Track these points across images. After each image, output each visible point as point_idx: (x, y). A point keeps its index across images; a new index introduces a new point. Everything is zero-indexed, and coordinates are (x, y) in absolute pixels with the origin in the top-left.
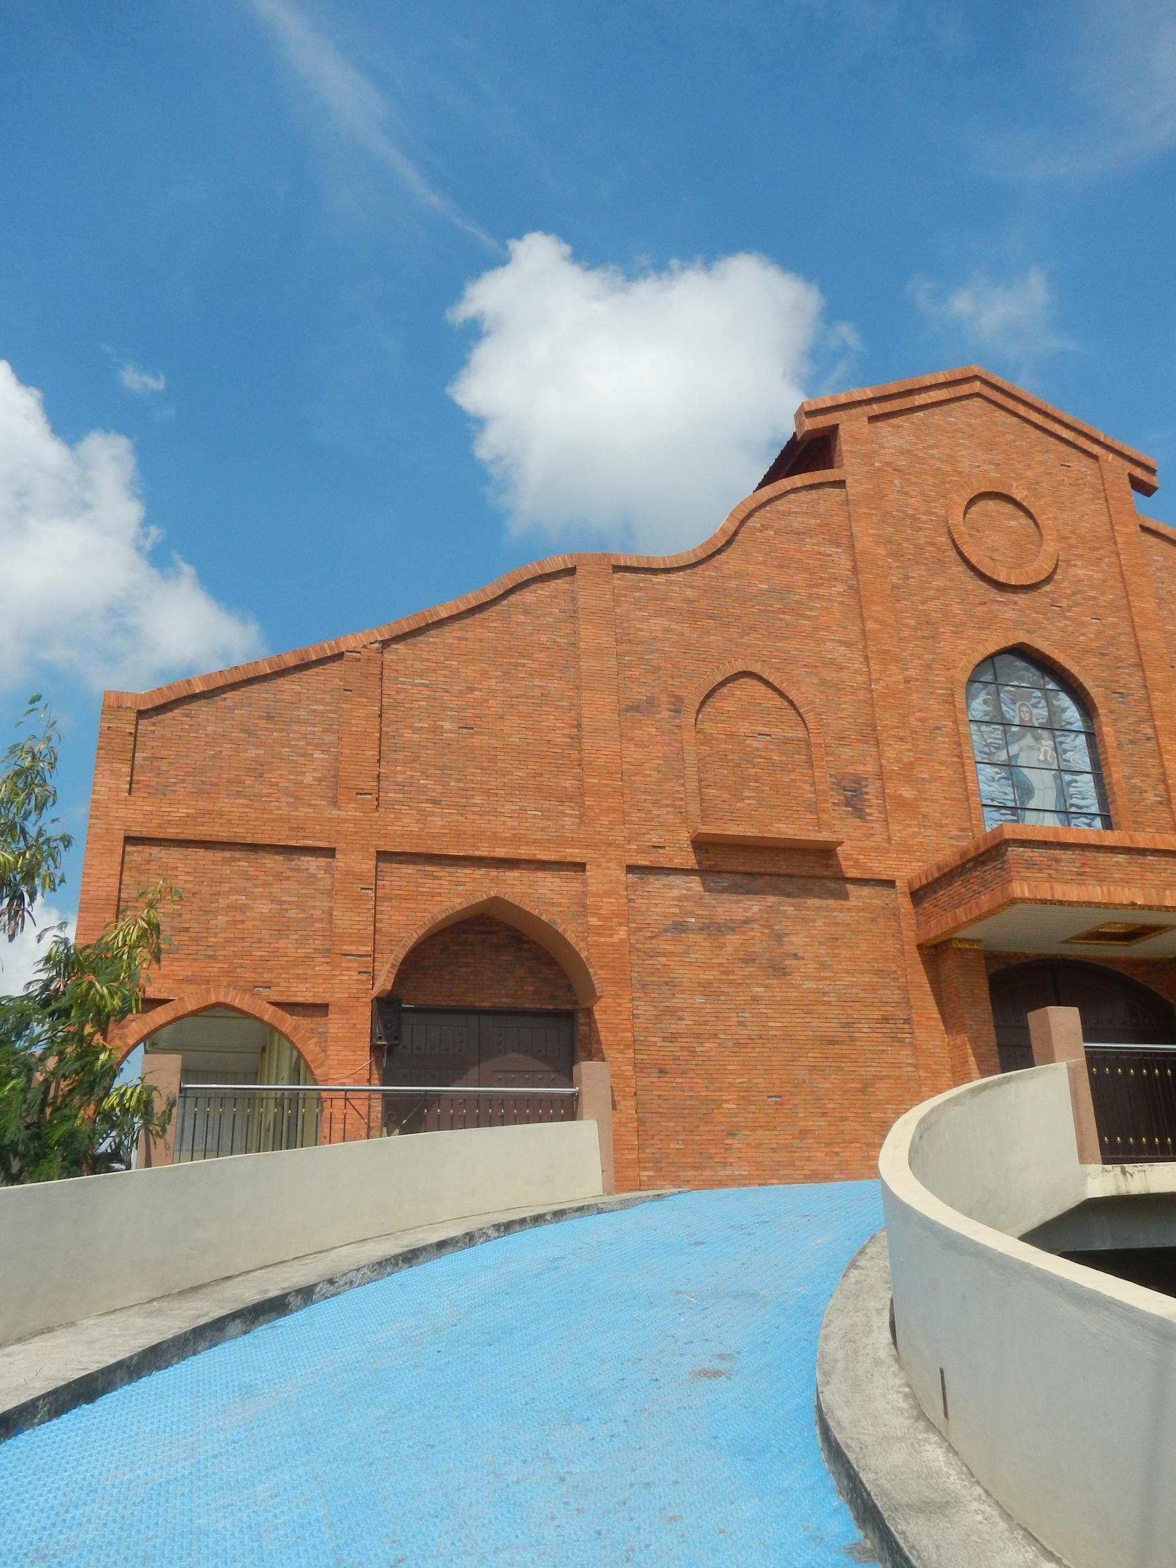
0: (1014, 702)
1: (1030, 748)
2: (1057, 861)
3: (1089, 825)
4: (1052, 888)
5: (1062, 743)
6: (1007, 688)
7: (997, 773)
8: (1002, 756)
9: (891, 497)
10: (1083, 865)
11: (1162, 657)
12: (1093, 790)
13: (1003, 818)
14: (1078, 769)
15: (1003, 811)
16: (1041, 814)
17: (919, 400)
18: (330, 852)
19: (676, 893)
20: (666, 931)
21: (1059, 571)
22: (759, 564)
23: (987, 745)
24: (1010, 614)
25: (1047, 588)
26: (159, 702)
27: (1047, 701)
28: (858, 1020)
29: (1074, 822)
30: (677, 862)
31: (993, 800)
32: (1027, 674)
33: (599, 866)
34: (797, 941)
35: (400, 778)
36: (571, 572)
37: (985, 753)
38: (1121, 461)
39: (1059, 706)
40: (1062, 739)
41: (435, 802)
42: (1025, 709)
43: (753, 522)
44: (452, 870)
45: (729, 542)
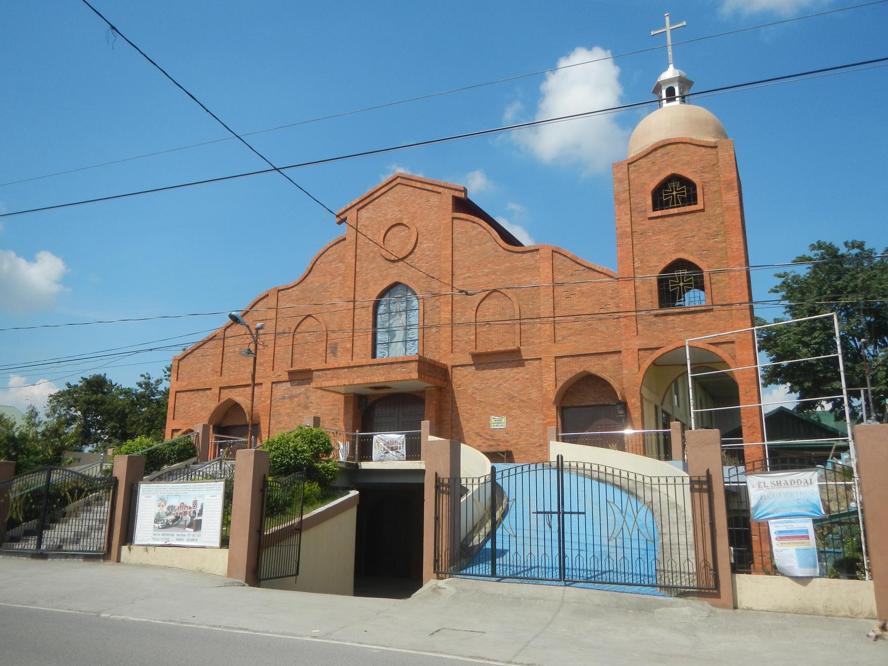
0: (395, 303)
1: (397, 319)
2: (326, 374)
3: (413, 344)
4: (321, 384)
5: (409, 315)
8: (388, 324)
9: (362, 238)
10: (334, 374)
11: (449, 273)
17: (376, 195)
18: (210, 389)
19: (283, 388)
20: (280, 399)
21: (417, 248)
22: (318, 277)
24: (395, 271)
25: (410, 256)
26: (182, 357)
28: (326, 420)
29: (408, 344)
30: (284, 380)
32: (401, 291)
33: (265, 383)
34: (313, 398)
35: (226, 366)
36: (267, 295)
38: (451, 191)
40: (409, 314)
41: (233, 371)
42: (398, 305)
43: (318, 262)
44: (235, 389)
45: (310, 272)
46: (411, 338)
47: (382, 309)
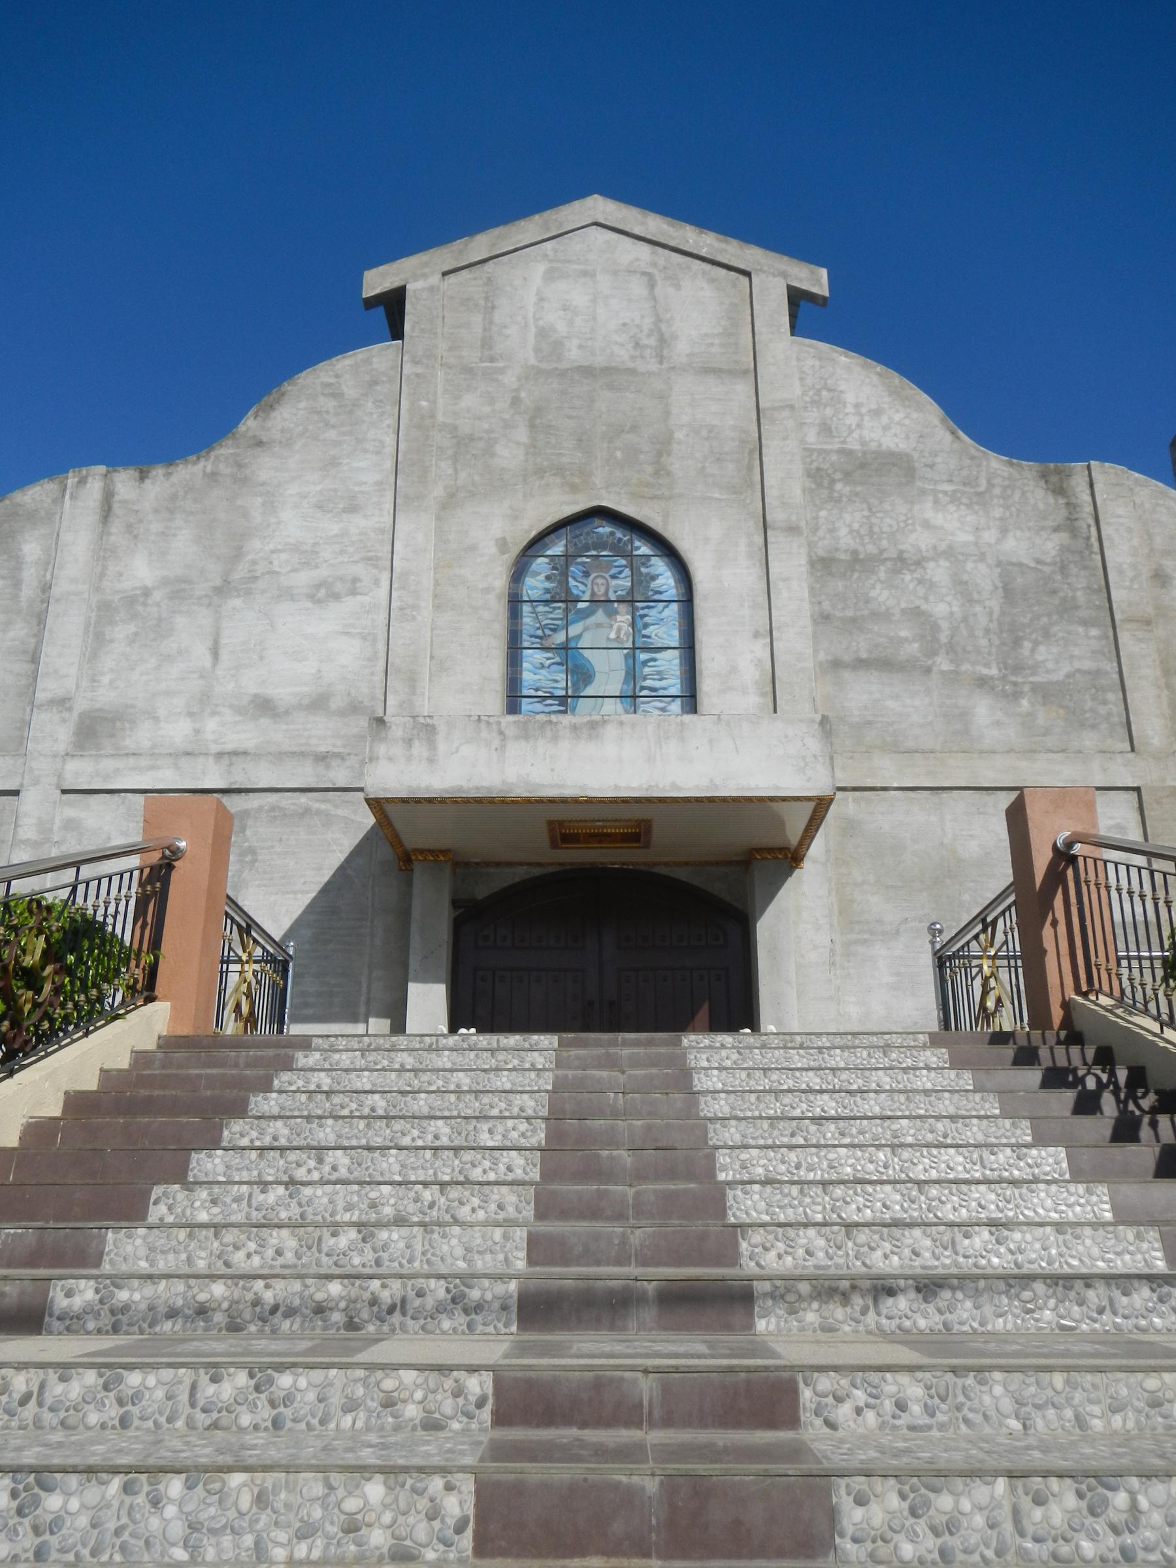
0: (586, 574)
1: (599, 625)
3: (663, 710)
6: (579, 560)
7: (548, 659)
8: (560, 638)
12: (678, 668)
13: (547, 709)
14: (659, 645)
15: (549, 702)
23: (542, 628)
27: (632, 570)
31: (537, 690)
37: (537, 637)
39: (648, 574)
40: (646, 611)
42: (600, 581)
47: (535, 585)
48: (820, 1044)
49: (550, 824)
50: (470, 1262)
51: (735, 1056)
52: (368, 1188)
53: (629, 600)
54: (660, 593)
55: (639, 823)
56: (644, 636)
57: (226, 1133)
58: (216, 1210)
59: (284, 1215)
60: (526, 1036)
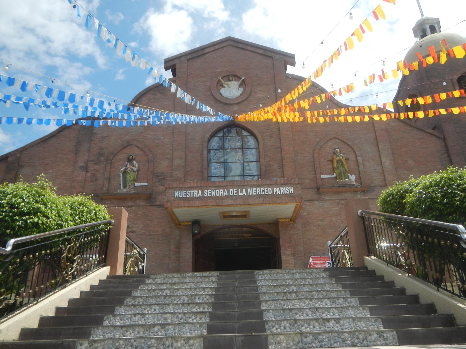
0: (229, 141)
8: (222, 160)
12: (255, 167)
15: (219, 178)
16: (234, 177)
31: (216, 175)
42: (233, 143)
46: (250, 173)
48: (293, 272)
49: (220, 213)
50: (191, 333)
51: (269, 276)
52: (163, 315)
53: (242, 148)
54: (250, 146)
55: (246, 212)
56: (246, 158)
57: (125, 302)
58: (122, 322)
59: (140, 323)
60: (210, 272)
